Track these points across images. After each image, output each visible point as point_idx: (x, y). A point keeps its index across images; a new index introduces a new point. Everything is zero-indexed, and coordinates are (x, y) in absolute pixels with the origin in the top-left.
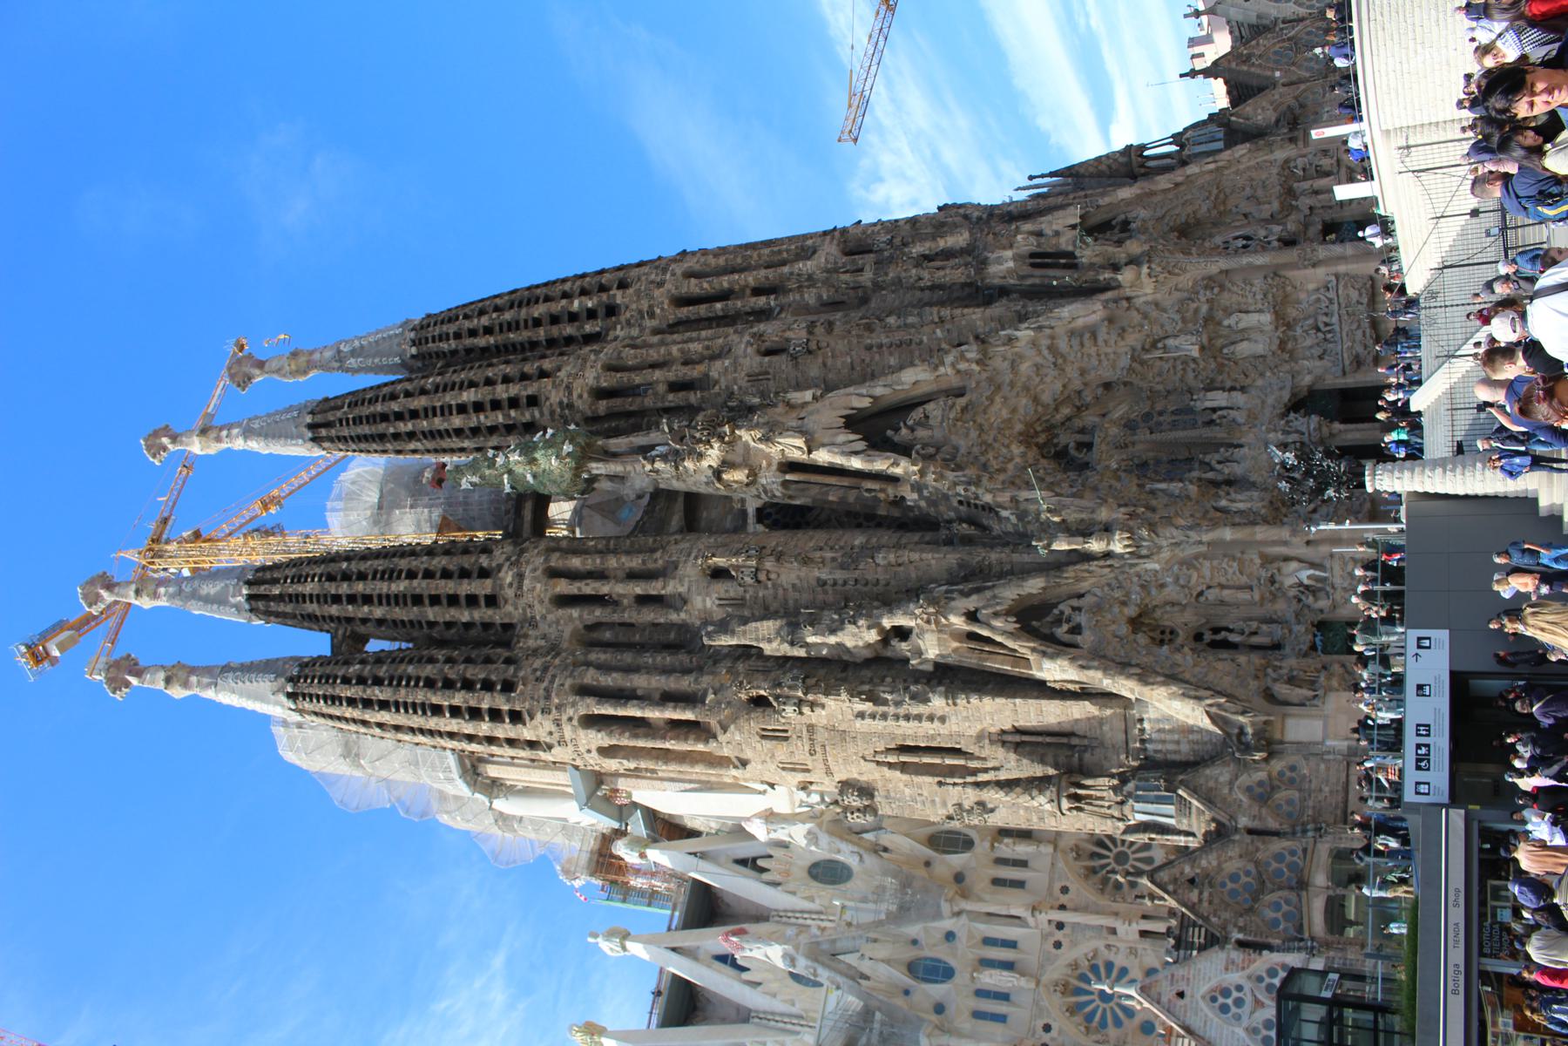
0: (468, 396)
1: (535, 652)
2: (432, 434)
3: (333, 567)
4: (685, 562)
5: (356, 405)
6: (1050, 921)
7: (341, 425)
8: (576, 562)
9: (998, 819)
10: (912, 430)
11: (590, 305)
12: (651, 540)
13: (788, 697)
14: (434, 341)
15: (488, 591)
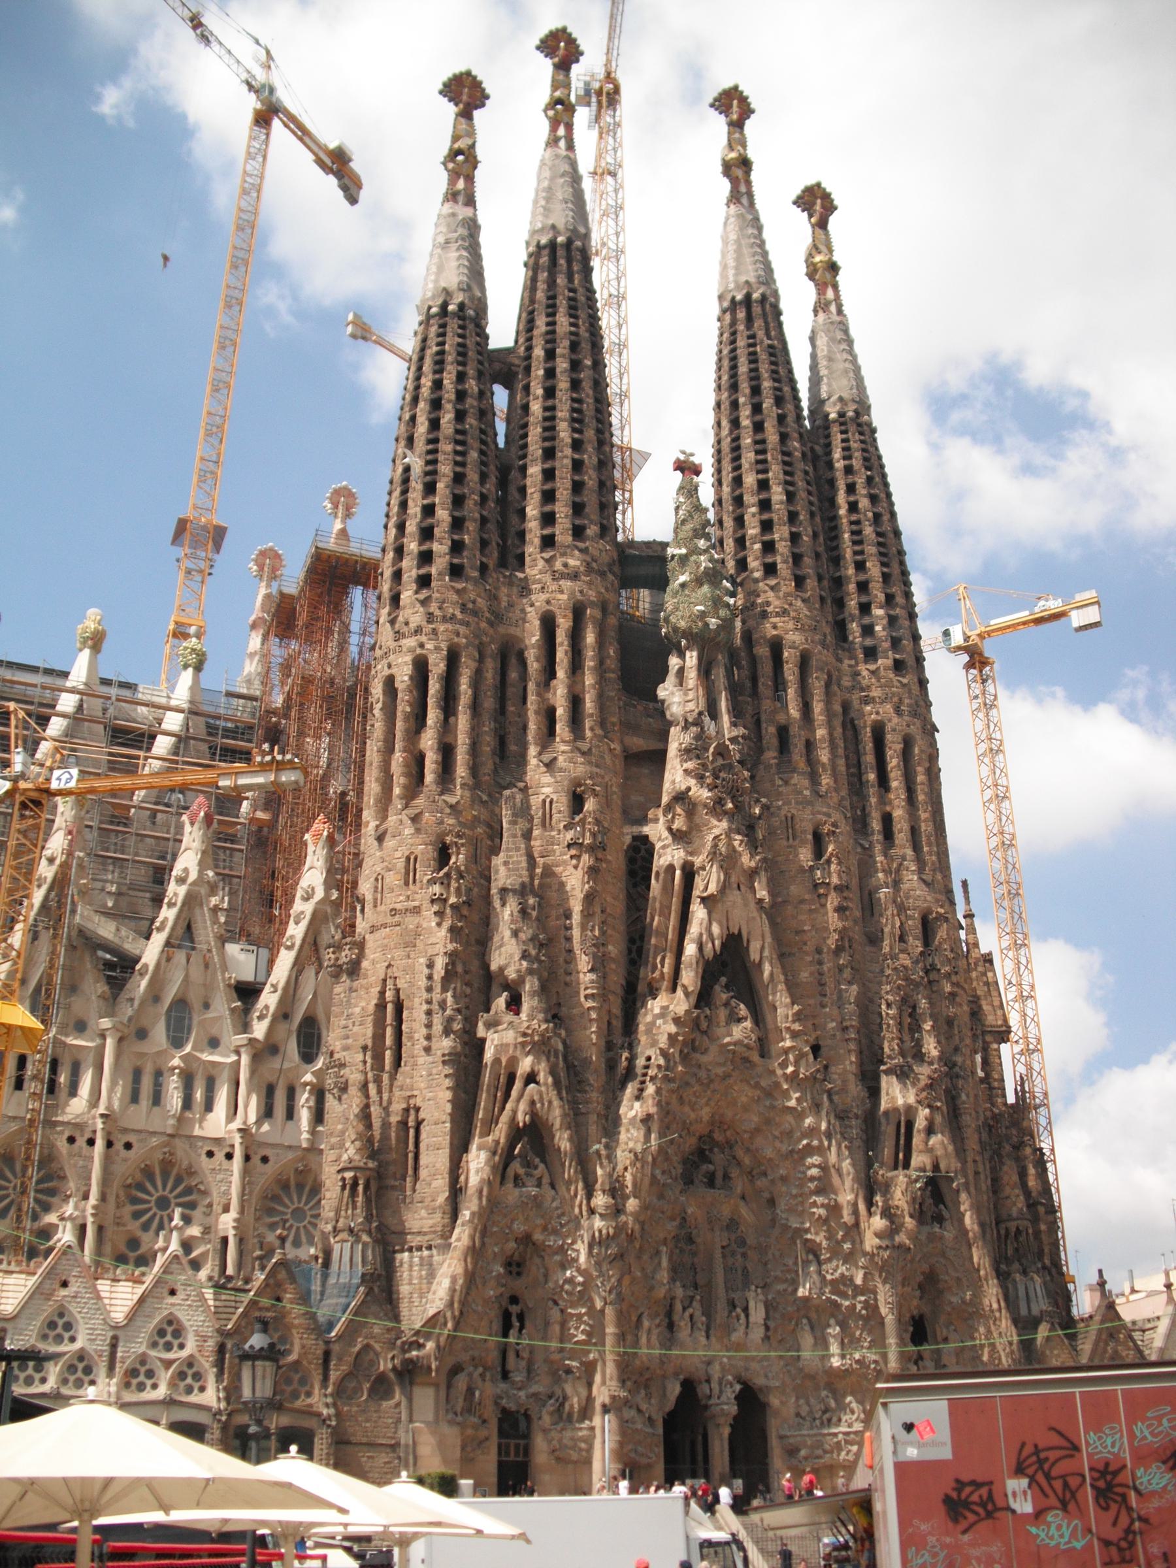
0: (777, 494)
1: (493, 597)
2: (736, 449)
3: (585, 346)
4: (590, 763)
5: (771, 355)
6: (233, 1146)
7: (749, 337)
8: (590, 638)
9: (330, 1102)
10: (726, 1004)
11: (878, 628)
12: (614, 720)
13: (449, 885)
14: (843, 441)
15: (558, 538)
